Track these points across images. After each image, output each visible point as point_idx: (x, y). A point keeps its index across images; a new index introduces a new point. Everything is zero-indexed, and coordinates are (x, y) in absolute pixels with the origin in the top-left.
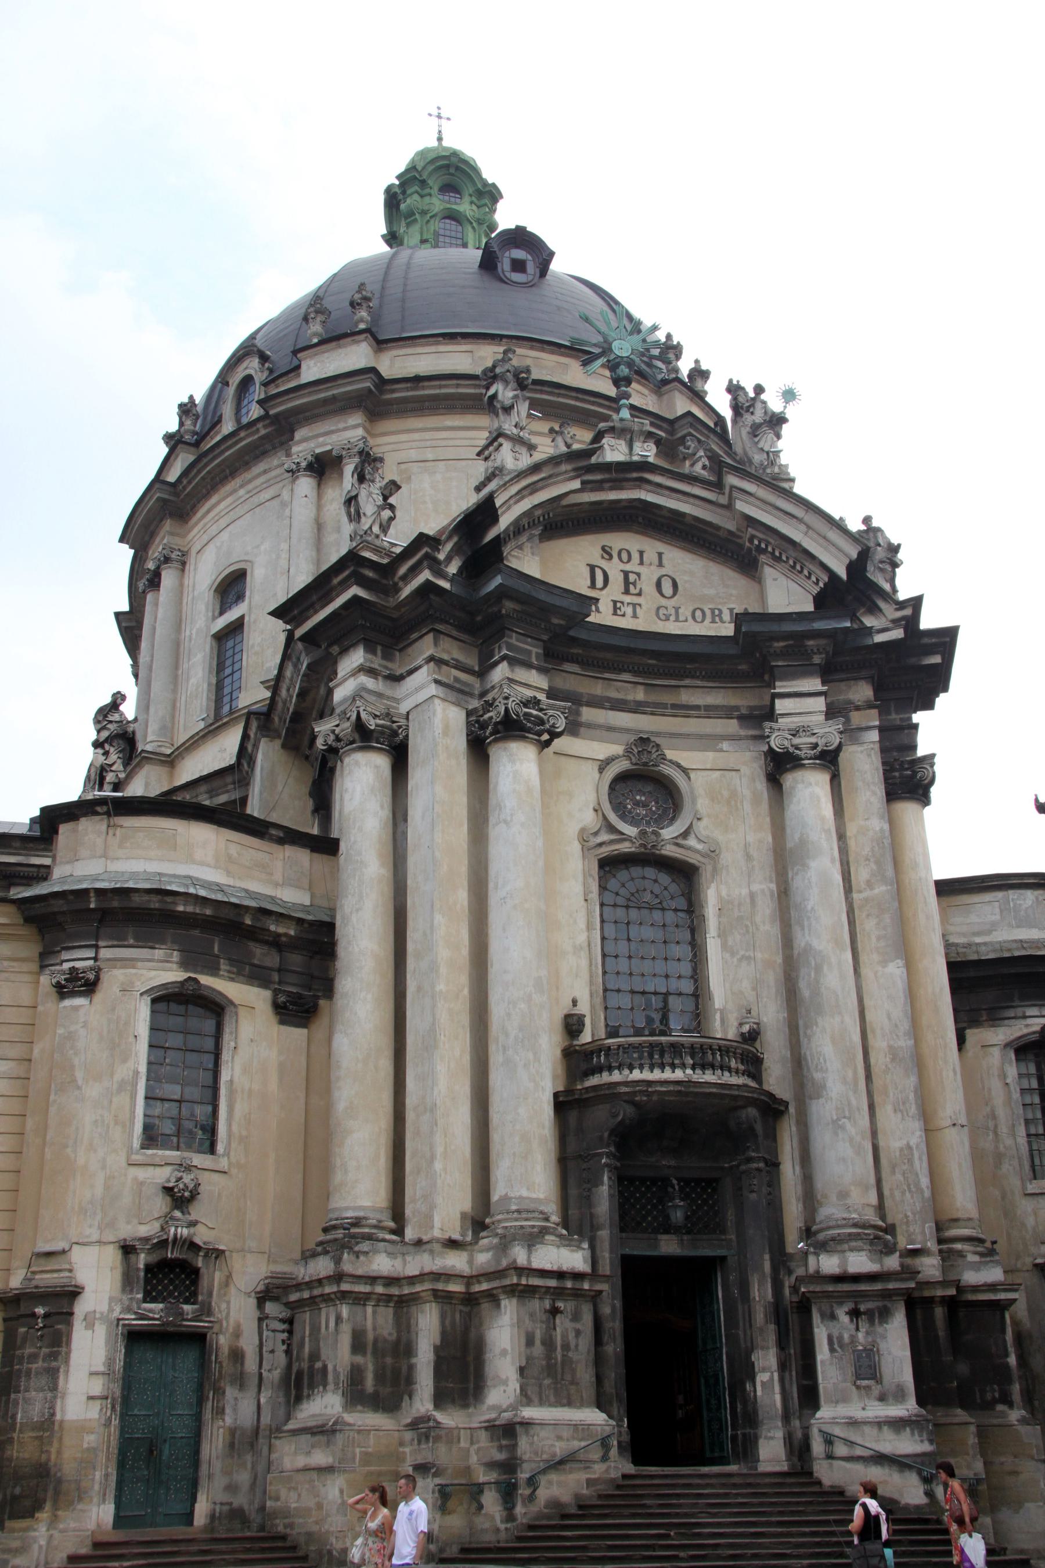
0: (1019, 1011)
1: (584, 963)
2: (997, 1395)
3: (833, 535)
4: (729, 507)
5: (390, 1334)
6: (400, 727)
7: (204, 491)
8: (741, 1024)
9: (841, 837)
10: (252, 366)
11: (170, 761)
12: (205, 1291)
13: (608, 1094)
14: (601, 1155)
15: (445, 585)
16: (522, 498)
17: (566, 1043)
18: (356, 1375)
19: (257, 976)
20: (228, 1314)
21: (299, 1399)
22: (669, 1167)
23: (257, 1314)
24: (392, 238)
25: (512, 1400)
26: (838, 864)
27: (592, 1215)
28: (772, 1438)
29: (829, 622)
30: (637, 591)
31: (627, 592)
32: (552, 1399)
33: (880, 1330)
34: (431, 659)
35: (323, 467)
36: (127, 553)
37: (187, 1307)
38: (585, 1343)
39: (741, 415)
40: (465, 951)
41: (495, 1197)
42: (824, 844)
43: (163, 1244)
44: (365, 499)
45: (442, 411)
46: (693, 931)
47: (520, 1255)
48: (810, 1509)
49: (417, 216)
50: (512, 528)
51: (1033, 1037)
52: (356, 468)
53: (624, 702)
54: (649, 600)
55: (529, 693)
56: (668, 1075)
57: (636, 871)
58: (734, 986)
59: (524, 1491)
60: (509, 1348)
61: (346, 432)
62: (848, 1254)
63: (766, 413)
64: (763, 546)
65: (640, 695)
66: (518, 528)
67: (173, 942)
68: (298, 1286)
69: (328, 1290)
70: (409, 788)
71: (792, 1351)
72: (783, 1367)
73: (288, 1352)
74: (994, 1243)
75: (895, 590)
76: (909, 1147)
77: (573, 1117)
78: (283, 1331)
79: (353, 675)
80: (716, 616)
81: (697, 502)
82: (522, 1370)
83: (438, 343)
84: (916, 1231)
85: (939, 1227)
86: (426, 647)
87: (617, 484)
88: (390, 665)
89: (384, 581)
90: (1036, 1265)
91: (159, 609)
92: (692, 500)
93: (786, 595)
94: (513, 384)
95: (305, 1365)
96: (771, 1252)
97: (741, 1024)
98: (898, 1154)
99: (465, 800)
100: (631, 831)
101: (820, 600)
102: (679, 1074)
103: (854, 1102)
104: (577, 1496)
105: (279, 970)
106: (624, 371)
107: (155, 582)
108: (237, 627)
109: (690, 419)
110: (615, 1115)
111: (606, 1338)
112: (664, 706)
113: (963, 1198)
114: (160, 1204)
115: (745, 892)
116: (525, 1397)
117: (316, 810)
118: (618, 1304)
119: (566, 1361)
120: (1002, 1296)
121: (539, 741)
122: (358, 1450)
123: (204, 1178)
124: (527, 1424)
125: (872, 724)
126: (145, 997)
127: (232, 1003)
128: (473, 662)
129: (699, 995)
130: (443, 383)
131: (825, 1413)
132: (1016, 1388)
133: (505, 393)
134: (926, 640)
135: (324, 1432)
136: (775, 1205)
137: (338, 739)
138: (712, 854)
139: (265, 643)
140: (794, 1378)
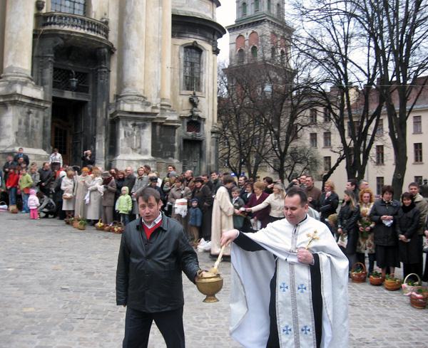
0: (187, 35)
8: (102, 19)
13: (54, 34)
14: (49, 57)
17: (36, 12)
25: (11, 144)
32: (27, 145)
33: (142, 131)
38: (40, 126)
47: (18, 89)
51: (191, 45)
56: (78, 30)
60: (11, 124)
72: (106, 140)
76: (155, 72)
82: (16, 133)
84: (155, 101)
97: (102, 19)
102: (82, 31)
110: (55, 42)
113: (167, 93)
119: (33, 132)
120: (176, 124)
131: (120, 157)
132: (176, 153)
136: (108, 85)
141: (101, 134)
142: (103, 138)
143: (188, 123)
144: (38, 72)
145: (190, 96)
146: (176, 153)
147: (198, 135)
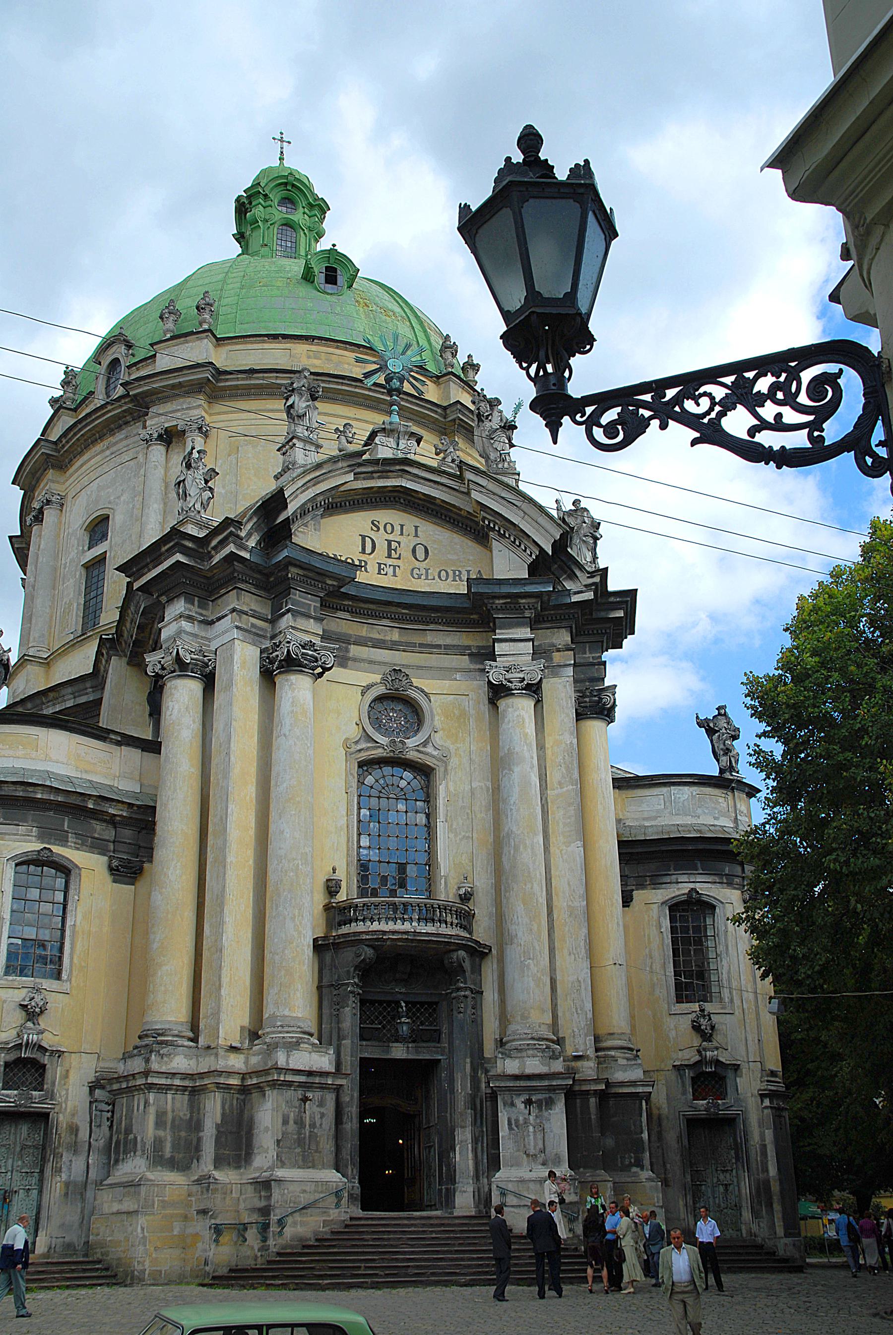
1: (344, 840)
2: (633, 1161)
3: (542, 520)
4: (468, 494)
5: (185, 1115)
6: (210, 660)
7: (79, 449)
9: (541, 747)
10: (119, 351)
11: (47, 663)
12: (49, 1081)
13: (354, 941)
14: (347, 984)
15: (246, 555)
16: (308, 488)
18: (158, 1143)
19: (97, 846)
20: (67, 1097)
21: (117, 1161)
23: (88, 1099)
24: (240, 237)
25: (270, 1164)
26: (536, 769)
27: (339, 1029)
28: (465, 1192)
29: (537, 586)
30: (397, 556)
31: (389, 556)
32: (301, 1163)
33: (545, 1114)
34: (234, 610)
35: (170, 437)
36: (18, 493)
37: (34, 1093)
39: (483, 422)
40: (252, 832)
41: (266, 1016)
42: (527, 755)
43: (19, 1047)
44: (190, 482)
45: (264, 397)
46: (428, 816)
47: (281, 1059)
48: (483, 1241)
49: (260, 223)
50: (299, 511)
52: (184, 458)
53: (384, 641)
54: (406, 562)
55: (307, 638)
57: (387, 770)
58: (456, 857)
59: (274, 1228)
61: (189, 410)
62: (526, 1059)
63: (501, 420)
64: (492, 525)
65: (395, 636)
66: (303, 511)
67: (32, 821)
68: (118, 1079)
69: (140, 1081)
70: (215, 707)
72: (475, 1140)
73: (111, 1127)
74: (638, 1051)
75: (595, 558)
76: (579, 982)
78: (108, 1111)
79: (176, 620)
80: (457, 576)
81: (444, 489)
83: (264, 342)
84: (579, 1042)
85: (597, 1039)
86: (232, 600)
87: (384, 474)
88: (204, 612)
89: (201, 550)
90: (674, 1066)
91: (43, 539)
92: (441, 487)
93: (508, 565)
94: (307, 396)
95: (122, 1137)
97: (459, 888)
98: (570, 985)
99: (257, 717)
100: (383, 740)
101: (533, 569)
102: (407, 926)
103: (537, 948)
104: (315, 1233)
105: (114, 842)
106: (396, 383)
107: (39, 518)
108: (101, 560)
109: (459, 406)
111: (345, 1119)
112: (414, 645)
114: (19, 1016)
115: (467, 788)
116: (281, 1162)
117: (150, 715)
118: (356, 1094)
119: (313, 1136)
120: (640, 1090)
121: (312, 674)
122: (156, 1199)
123: (51, 997)
124: (279, 1181)
125: (568, 663)
126: (10, 862)
127: (77, 866)
128: (267, 612)
129: (431, 862)
130: (266, 375)
133: (301, 403)
134: (612, 599)
135: (133, 1185)
136: (477, 1023)
137: (163, 668)
138: (444, 759)
139: (115, 586)
142: (469, 1136)
143: (694, 1080)
144: (331, 1015)
145: (694, 1015)
146: (647, 1162)
147: (725, 1106)
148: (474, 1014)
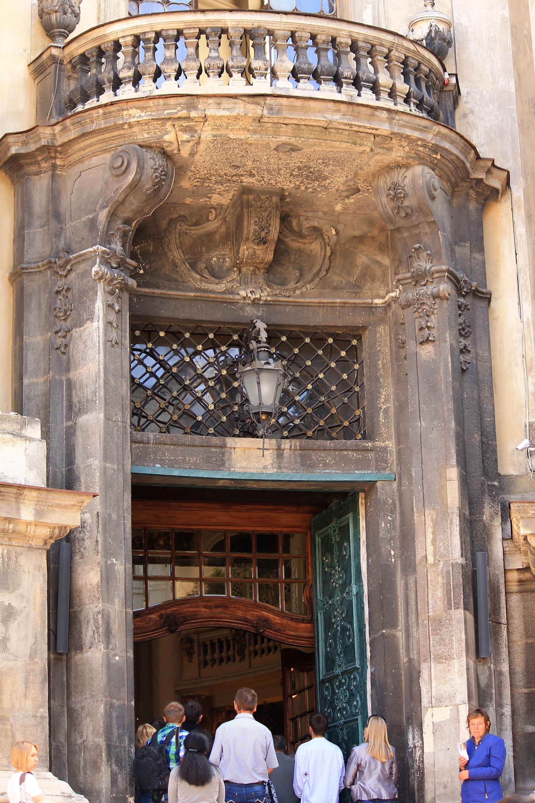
22: (255, 303)
27: (70, 384)
71: (505, 668)
77: (40, 187)
96: (463, 463)
97: (412, 25)
111: (88, 633)
140: (508, 721)
141: (444, 658)
148: (464, 350)
